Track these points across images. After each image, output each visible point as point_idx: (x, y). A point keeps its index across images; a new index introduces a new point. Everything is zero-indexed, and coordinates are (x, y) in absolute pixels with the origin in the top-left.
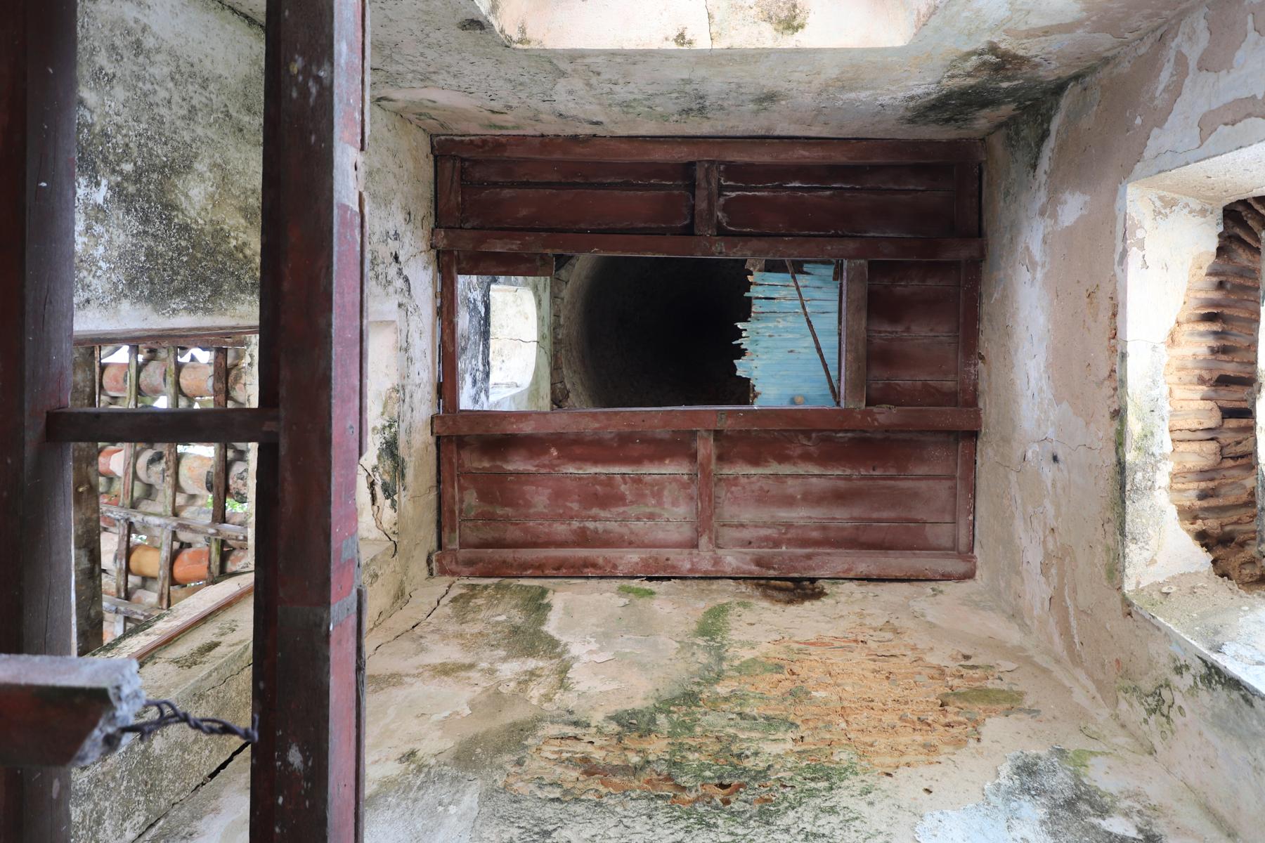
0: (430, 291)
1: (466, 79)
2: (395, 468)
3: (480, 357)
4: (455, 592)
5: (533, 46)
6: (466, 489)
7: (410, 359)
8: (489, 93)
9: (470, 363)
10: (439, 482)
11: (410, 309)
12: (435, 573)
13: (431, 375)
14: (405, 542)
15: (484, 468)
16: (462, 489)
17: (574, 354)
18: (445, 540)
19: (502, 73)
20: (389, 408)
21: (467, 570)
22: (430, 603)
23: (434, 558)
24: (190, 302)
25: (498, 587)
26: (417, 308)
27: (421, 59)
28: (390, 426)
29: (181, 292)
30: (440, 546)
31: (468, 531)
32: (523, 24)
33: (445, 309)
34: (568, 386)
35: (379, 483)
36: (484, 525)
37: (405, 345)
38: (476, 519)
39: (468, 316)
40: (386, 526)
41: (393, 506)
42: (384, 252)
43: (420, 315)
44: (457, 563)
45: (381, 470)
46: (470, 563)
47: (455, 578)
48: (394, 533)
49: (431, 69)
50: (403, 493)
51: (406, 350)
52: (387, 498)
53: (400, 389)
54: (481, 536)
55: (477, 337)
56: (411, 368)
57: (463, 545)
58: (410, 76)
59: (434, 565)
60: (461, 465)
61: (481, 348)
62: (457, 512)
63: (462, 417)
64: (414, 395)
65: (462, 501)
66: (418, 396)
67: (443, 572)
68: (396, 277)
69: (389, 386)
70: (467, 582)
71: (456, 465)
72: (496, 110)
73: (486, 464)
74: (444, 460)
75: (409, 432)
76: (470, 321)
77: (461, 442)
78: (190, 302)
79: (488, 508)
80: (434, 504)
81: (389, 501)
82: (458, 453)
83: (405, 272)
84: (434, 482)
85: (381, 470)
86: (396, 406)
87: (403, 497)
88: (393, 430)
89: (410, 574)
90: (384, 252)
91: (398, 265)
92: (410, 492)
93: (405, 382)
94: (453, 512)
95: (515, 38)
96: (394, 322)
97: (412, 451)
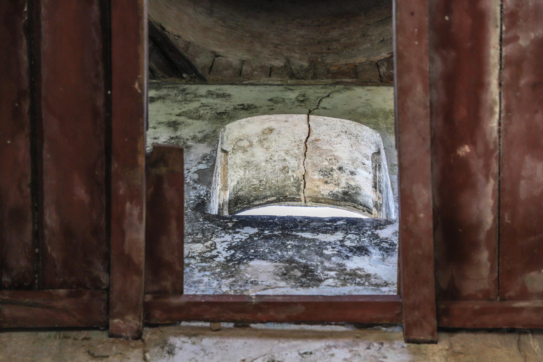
3: (322, 237)
9: (329, 258)
13: (341, 342)
33: (238, 317)
39: (255, 263)
60: (486, 295)
61: (308, 235)
76: (263, 257)
82: (468, 298)
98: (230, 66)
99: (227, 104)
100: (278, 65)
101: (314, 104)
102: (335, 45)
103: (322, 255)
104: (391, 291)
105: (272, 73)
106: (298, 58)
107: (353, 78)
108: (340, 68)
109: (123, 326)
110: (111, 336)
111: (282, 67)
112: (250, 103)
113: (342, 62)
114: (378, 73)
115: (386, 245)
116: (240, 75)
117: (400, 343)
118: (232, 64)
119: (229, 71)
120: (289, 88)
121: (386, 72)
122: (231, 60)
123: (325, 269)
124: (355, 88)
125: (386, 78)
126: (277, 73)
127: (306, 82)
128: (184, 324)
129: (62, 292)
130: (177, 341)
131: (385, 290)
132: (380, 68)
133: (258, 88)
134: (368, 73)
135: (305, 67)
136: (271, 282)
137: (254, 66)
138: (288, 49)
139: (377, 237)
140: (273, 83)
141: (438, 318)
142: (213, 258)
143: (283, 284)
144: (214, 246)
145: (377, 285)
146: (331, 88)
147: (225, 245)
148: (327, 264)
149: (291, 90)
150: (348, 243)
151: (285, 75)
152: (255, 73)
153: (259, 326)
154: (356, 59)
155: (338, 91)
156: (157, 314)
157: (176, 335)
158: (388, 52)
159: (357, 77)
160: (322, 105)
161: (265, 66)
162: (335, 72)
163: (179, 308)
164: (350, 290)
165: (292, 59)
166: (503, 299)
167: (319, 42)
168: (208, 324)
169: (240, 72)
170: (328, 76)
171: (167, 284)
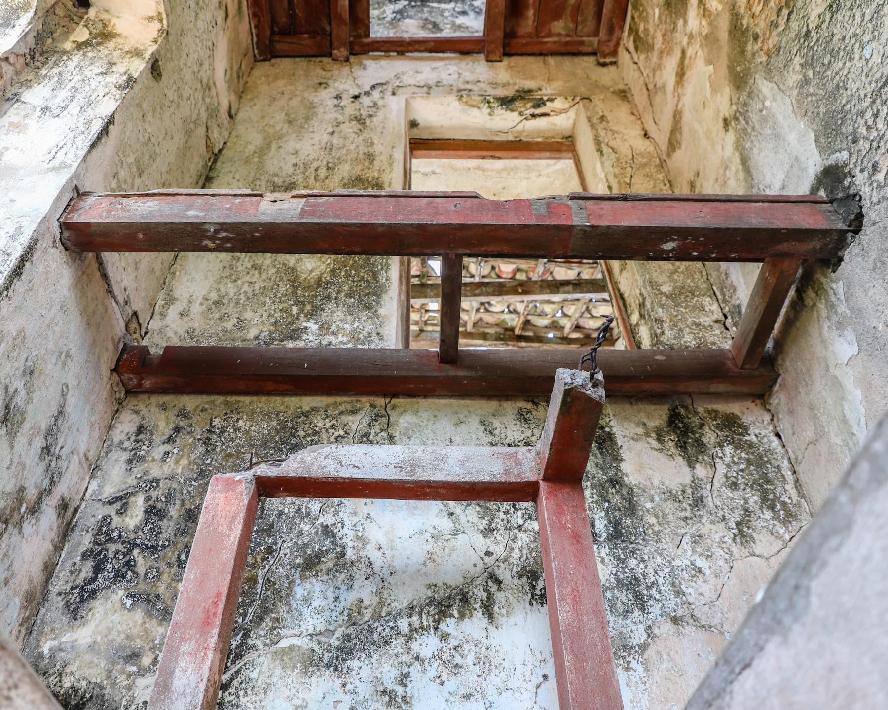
0: (384, 62)
1: (202, 54)
2: (523, 98)
4: (631, 46)
5: (162, 9)
6: (550, 30)
7: (438, 84)
8: (211, 28)
9: (446, 18)
10: (541, 54)
11: (397, 84)
12: (613, 60)
13: (453, 62)
14: (583, 89)
15: (534, 15)
16: (549, 35)
18: (589, 50)
19: (191, 25)
20: (474, 103)
21: (617, 32)
22: (634, 70)
23: (602, 60)
24: (382, 269)
25: (635, 8)
26: (397, 77)
27: (192, 98)
28: (489, 102)
29: (375, 275)
30: (594, 54)
31: (585, 29)
32: (145, 19)
33: (399, 49)
35: (532, 111)
36: (582, 14)
37: (426, 89)
38: (576, 23)
39: (407, 21)
40: (567, 106)
41: (551, 100)
42: (351, 109)
43: (403, 73)
44: (609, 41)
45: (523, 109)
46: (611, 30)
47: (622, 43)
48: (573, 100)
49: (199, 86)
50: (544, 91)
51: (430, 88)
52: (545, 105)
53: (460, 94)
54: (591, 18)
55: (426, 10)
56: (445, 82)
57: (596, 34)
58: (208, 100)
59: (608, 60)
60: (530, 35)
62: (568, 39)
63: (488, 35)
64: (467, 79)
65: (559, 35)
66: (468, 76)
67: (614, 53)
68: (371, 97)
69: (457, 103)
70: (626, 33)
71: (528, 40)
72: (224, 15)
73: (531, 13)
74: (524, 50)
75: (494, 85)
76: (411, 17)
77: (510, 35)
78: (382, 269)
79: (568, 11)
80: (559, 59)
81: (548, 104)
82: (520, 37)
83: (367, 88)
84: (540, 59)
85: (523, 109)
86: (473, 97)
87: (547, 91)
88: (492, 100)
89: (609, 84)
90: (351, 109)
91: (362, 95)
92: (544, 84)
93: (455, 89)
94: (567, 43)
95: (158, 26)
96: (406, 100)
97: (511, 82)
103: (443, 16)
104: (481, 34)
109: (339, 54)
110: (333, 60)
115: (477, 10)
117: (483, 62)
123: (444, 23)
128: (371, 53)
129: (306, 36)
130: (368, 62)
131: (476, 34)
136: (416, 30)
139: (472, 5)
141: (504, 48)
142: (384, 18)
143: (422, 32)
144: (384, 12)
145: (472, 32)
147: (391, 11)
148: (446, 21)
150: (457, 9)
153: (410, 54)
156: (356, 48)
157: (367, 59)
163: (368, 44)
164: (458, 34)
166: (538, 37)
168: (383, 54)
171: (361, 31)
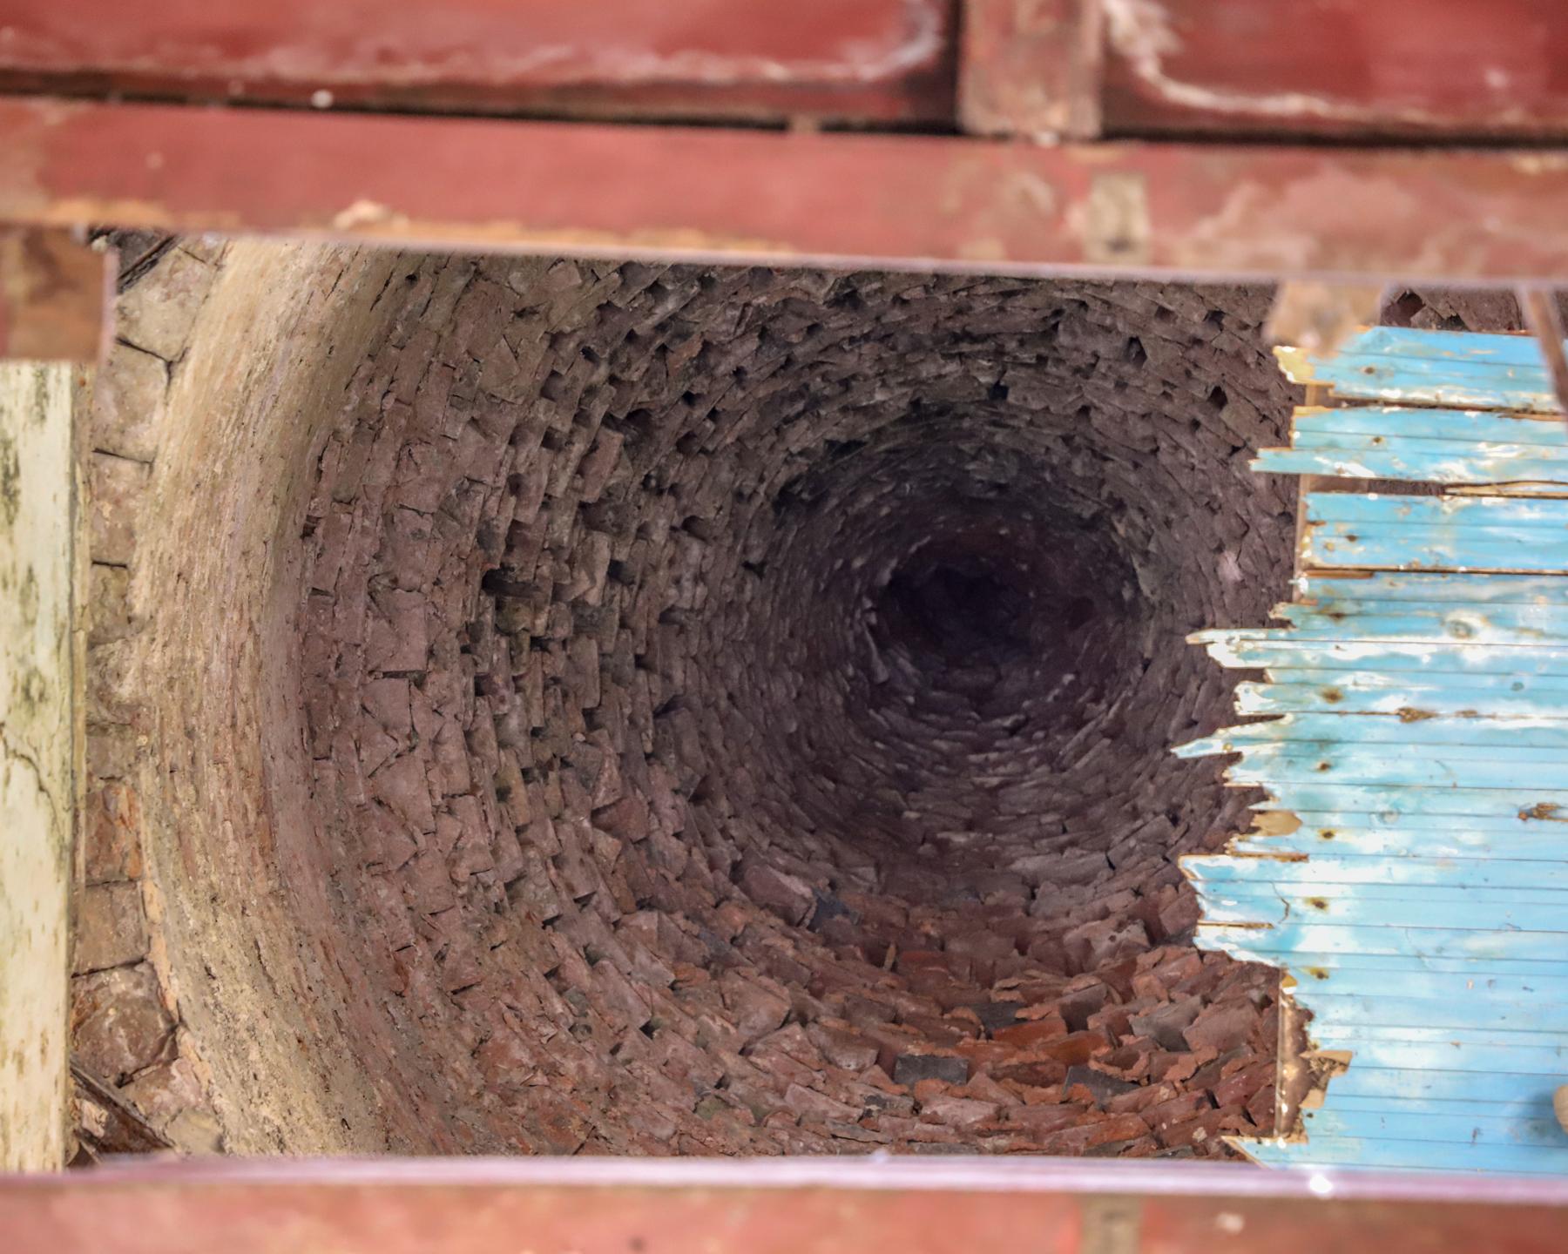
17: (214, 789)
34: (177, 989)
98: (134, 415)
99: (20, 416)
100: (136, 592)
101: (21, 738)
102: (185, 792)
105: (106, 571)
106: (148, 663)
107: (88, 872)
108: (124, 822)
111: (128, 606)
112: (23, 498)
113: (146, 829)
114: (104, 964)
116: (97, 451)
118: (143, 421)
119: (114, 411)
120: (66, 633)
121: (111, 995)
122: (157, 417)
124: (63, 883)
125: (88, 992)
126: (106, 589)
127: (80, 702)
132: (125, 972)
133: (63, 521)
134: (108, 925)
135: (115, 688)
137: (132, 503)
138: (173, 621)
140: (78, 575)
146: (65, 795)
149: (59, 647)
151: (98, 618)
152: (107, 509)
154: (157, 881)
155: (54, 820)
158: (183, 1002)
159: (91, 885)
160: (18, 768)
161: (134, 545)
162: (112, 807)
165: (145, 638)
167: (190, 734)
169: (111, 451)
170: (95, 779)
